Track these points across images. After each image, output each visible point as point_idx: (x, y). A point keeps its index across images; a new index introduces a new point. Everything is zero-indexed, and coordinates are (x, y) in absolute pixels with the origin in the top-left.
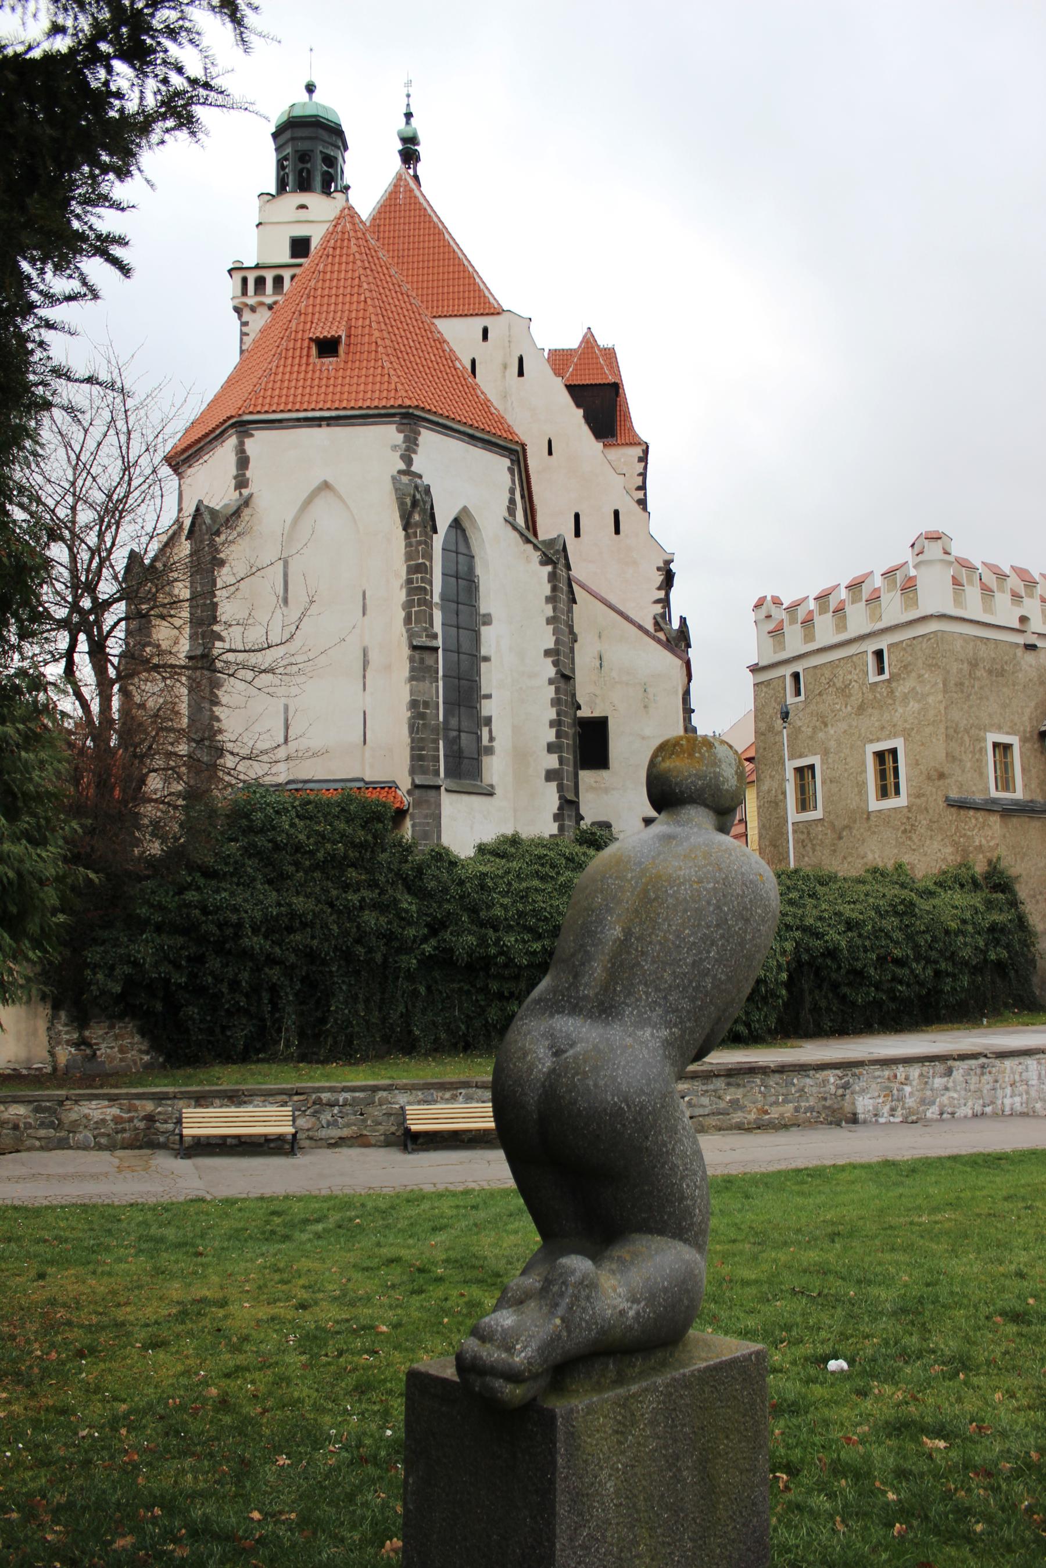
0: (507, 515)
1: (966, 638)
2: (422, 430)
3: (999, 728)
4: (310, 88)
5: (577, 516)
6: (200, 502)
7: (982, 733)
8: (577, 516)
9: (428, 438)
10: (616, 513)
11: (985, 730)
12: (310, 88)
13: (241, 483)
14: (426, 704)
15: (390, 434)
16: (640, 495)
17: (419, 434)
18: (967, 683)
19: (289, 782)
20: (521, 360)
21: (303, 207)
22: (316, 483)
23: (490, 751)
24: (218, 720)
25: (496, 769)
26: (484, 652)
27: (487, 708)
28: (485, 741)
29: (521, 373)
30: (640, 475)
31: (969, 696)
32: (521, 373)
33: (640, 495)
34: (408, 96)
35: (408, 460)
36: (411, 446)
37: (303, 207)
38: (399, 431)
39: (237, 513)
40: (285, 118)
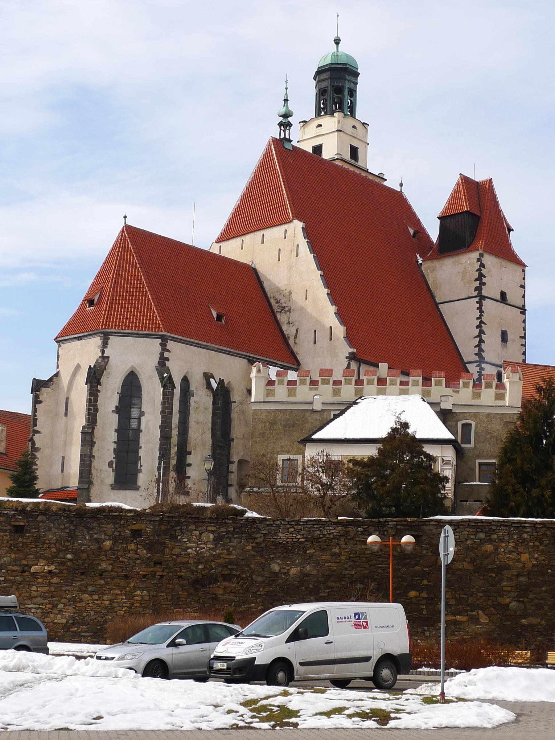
0: (157, 365)
1: (269, 412)
2: (110, 337)
3: (288, 452)
4: (337, 41)
5: (315, 331)
6: (34, 379)
7: (275, 456)
8: (315, 331)
9: (113, 340)
10: (331, 327)
11: (278, 454)
12: (337, 41)
13: (58, 367)
14: (85, 455)
15: (97, 341)
16: (477, 284)
17: (109, 339)
18: (267, 432)
19: (61, 488)
20: (298, 245)
21: (320, 125)
22: (76, 365)
23: (140, 471)
24: (36, 465)
25: (142, 479)
26: (141, 429)
27: (142, 453)
28: (139, 468)
29: (297, 255)
30: (477, 271)
31: (268, 439)
32: (297, 255)
33: (477, 284)
34: (286, 89)
35: (103, 352)
36: (105, 344)
37: (320, 125)
38: (101, 340)
39: (51, 380)
40: (328, 61)
